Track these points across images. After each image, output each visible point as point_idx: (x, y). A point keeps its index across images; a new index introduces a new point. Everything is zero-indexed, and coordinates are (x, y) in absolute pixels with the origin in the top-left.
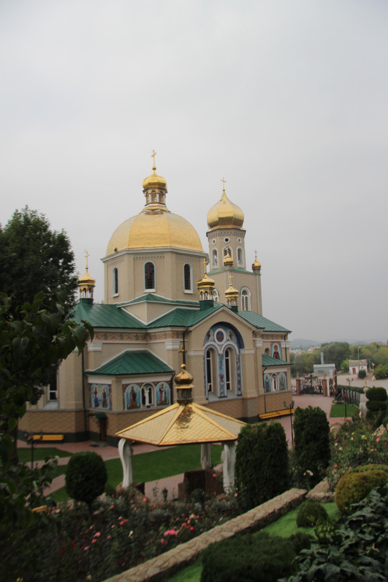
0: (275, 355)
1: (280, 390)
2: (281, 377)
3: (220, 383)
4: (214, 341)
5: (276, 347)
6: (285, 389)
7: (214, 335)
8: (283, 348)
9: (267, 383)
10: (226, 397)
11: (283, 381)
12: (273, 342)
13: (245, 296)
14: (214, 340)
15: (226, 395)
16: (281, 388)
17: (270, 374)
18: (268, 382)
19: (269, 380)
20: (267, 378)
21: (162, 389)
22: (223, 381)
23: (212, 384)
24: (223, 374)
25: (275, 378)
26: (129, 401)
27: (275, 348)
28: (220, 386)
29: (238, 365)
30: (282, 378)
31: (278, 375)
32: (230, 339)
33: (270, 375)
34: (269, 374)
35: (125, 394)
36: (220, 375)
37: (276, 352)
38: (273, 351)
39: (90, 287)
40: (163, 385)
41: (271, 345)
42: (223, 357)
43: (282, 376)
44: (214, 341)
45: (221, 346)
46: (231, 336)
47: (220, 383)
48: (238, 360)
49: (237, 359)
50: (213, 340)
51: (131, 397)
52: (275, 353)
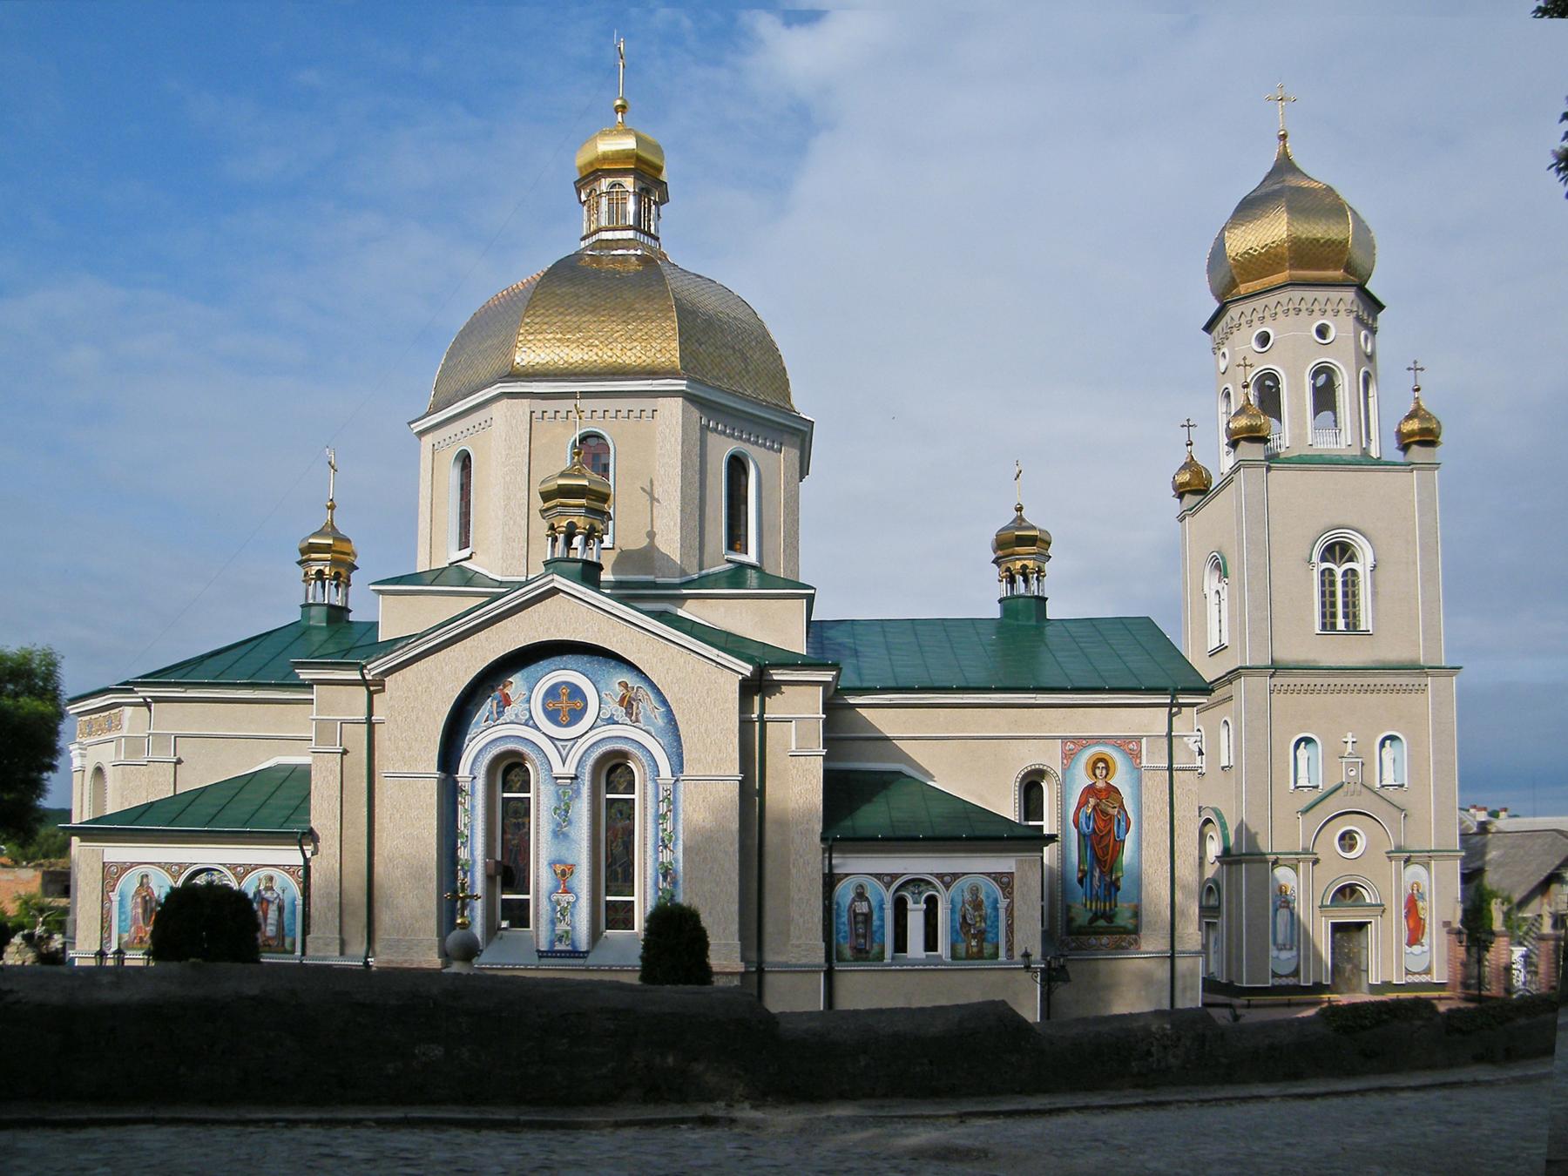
0: (1092, 801)
1: (954, 957)
2: (968, 897)
3: (555, 897)
4: (530, 722)
5: (1101, 764)
6: (995, 955)
7: (529, 701)
9: (860, 918)
10: (583, 955)
11: (983, 918)
12: (1082, 742)
13: (1339, 571)
14: (531, 717)
15: (583, 946)
16: (961, 948)
17: (887, 879)
18: (868, 917)
19: (874, 903)
20: (861, 896)
21: (268, 895)
22: (566, 892)
23: (531, 897)
24: (570, 861)
25: (932, 902)
26: (129, 922)
27: (1094, 767)
28: (554, 909)
29: (669, 826)
30: (977, 905)
31: (947, 886)
32: (620, 713)
33: (888, 886)
34: (878, 876)
35: (115, 897)
36: (552, 864)
37: (1100, 784)
38: (1082, 780)
39: (322, 568)
40: (271, 879)
41: (1069, 757)
42: (577, 792)
43: (975, 891)
44: (530, 722)
45: (572, 742)
46: (628, 703)
47: (555, 897)
48: (663, 808)
49: (658, 802)
50: (523, 719)
51: (135, 907)
52: (1090, 790)
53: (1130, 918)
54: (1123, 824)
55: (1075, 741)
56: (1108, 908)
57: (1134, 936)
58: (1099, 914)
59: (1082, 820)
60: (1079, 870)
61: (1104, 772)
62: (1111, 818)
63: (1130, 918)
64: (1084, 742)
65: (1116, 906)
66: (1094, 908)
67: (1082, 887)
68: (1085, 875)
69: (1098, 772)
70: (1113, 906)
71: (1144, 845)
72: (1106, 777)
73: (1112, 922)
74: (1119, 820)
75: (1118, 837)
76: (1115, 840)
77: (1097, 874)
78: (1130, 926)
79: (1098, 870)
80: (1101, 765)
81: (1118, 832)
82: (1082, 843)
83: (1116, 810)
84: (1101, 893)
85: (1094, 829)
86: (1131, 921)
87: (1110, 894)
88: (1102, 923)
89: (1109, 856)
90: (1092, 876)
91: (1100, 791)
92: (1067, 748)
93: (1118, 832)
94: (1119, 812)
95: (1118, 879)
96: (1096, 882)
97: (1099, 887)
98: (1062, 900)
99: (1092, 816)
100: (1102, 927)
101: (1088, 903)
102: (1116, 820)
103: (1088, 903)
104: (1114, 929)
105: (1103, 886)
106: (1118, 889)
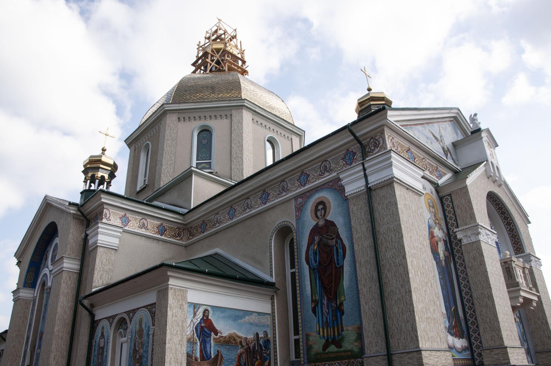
0: (317, 239)
8: (357, 196)
52: (315, 230)
53: (356, 341)
54: (341, 251)
55: (303, 196)
56: (336, 334)
57: (360, 360)
58: (330, 340)
59: (312, 257)
60: (312, 301)
61: (323, 212)
62: (331, 247)
63: (356, 341)
64: (308, 194)
65: (342, 330)
66: (325, 335)
67: (316, 317)
68: (316, 305)
69: (319, 214)
70: (340, 331)
71: (358, 265)
72: (324, 215)
73: (341, 347)
74: (337, 248)
75: (338, 264)
76: (336, 267)
77: (325, 302)
78: (356, 350)
79: (326, 298)
80: (320, 207)
81: (338, 260)
82: (313, 276)
83: (334, 240)
84: (330, 318)
85: (320, 262)
86: (356, 344)
87: (337, 320)
88: (332, 348)
89: (333, 284)
90: (322, 304)
91: (321, 228)
92: (298, 203)
93: (338, 260)
94: (336, 242)
95: (342, 304)
96: (325, 310)
97: (328, 314)
98: (302, 330)
99: (318, 252)
100: (332, 353)
101: (321, 329)
102: (335, 248)
103: (321, 329)
104: (343, 354)
105: (330, 311)
106: (342, 313)
